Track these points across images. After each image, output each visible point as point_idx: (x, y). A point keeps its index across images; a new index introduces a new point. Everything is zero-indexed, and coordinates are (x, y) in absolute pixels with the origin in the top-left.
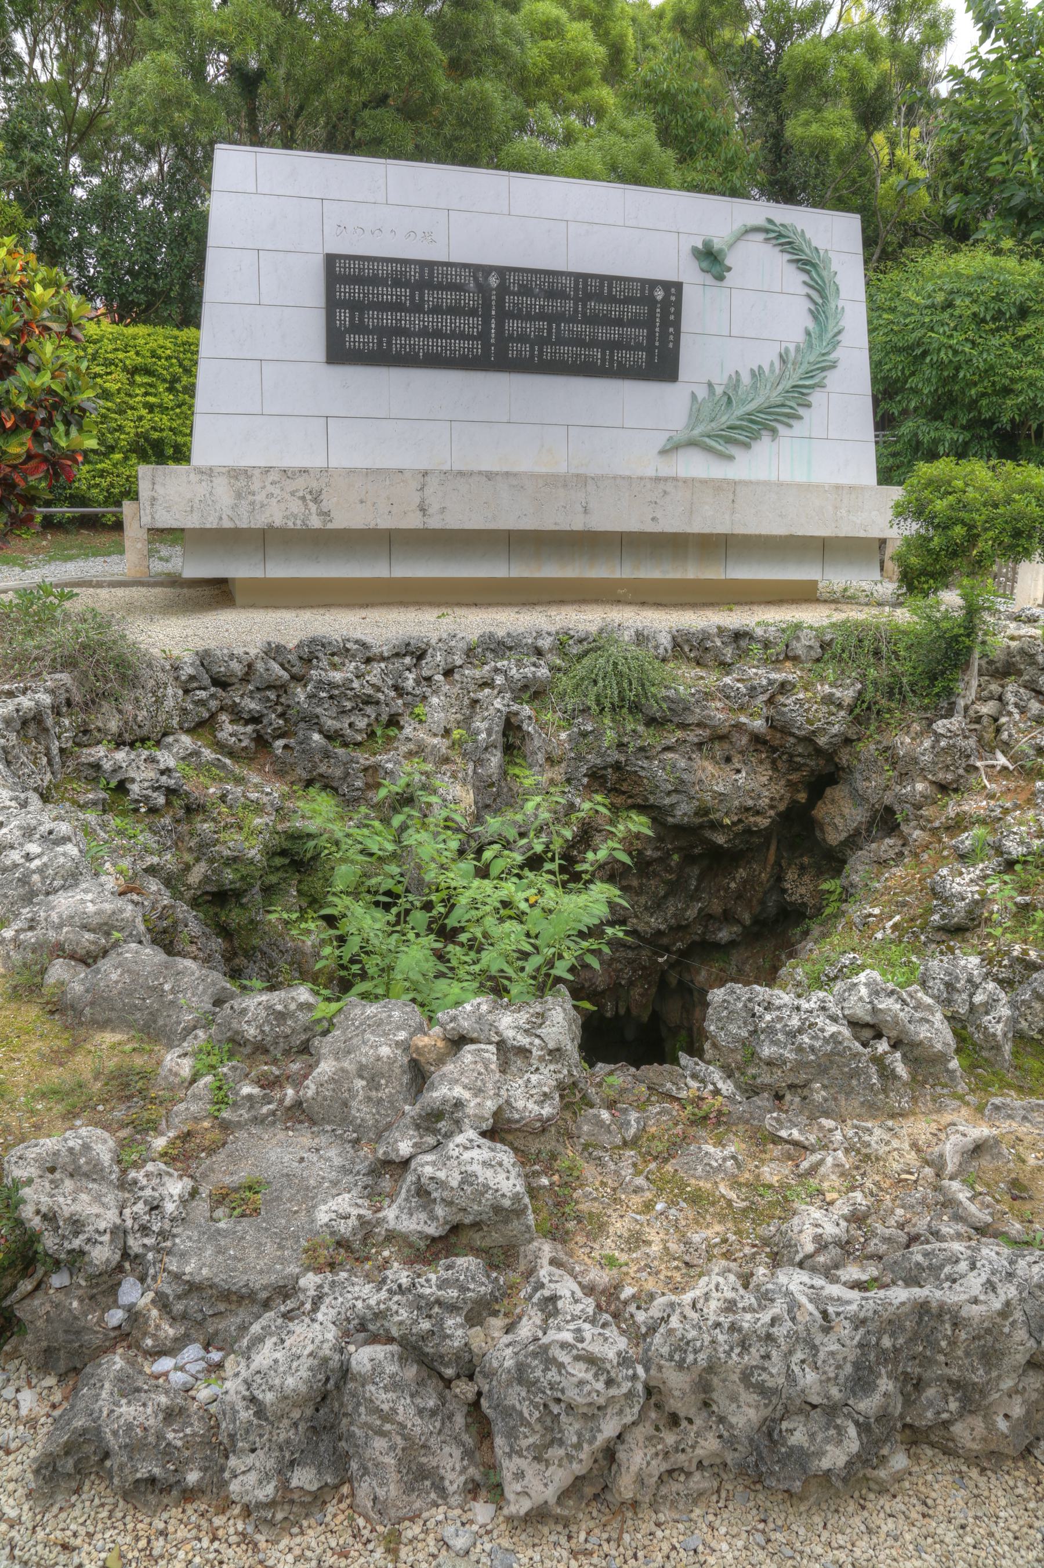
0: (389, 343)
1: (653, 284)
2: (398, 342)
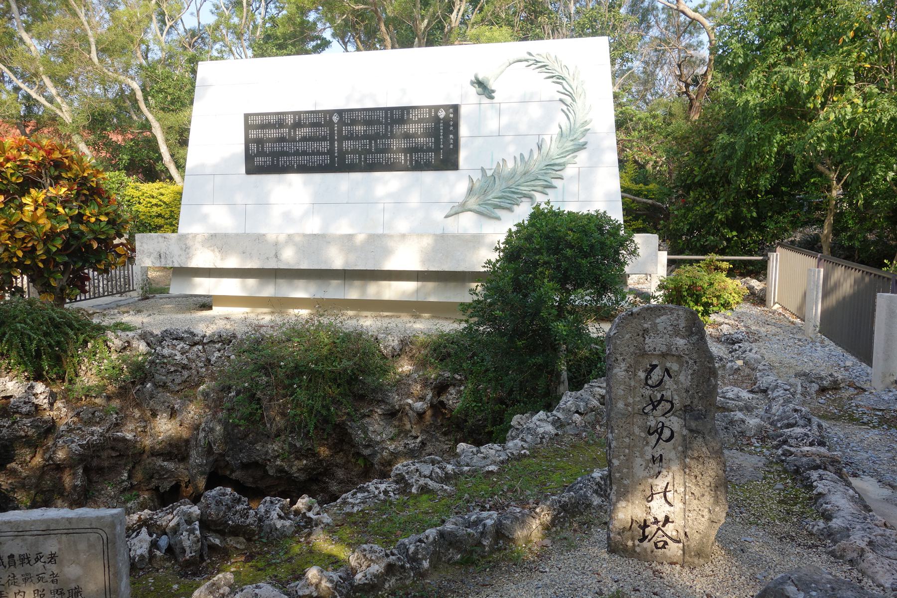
0: (278, 161)
2: (283, 160)
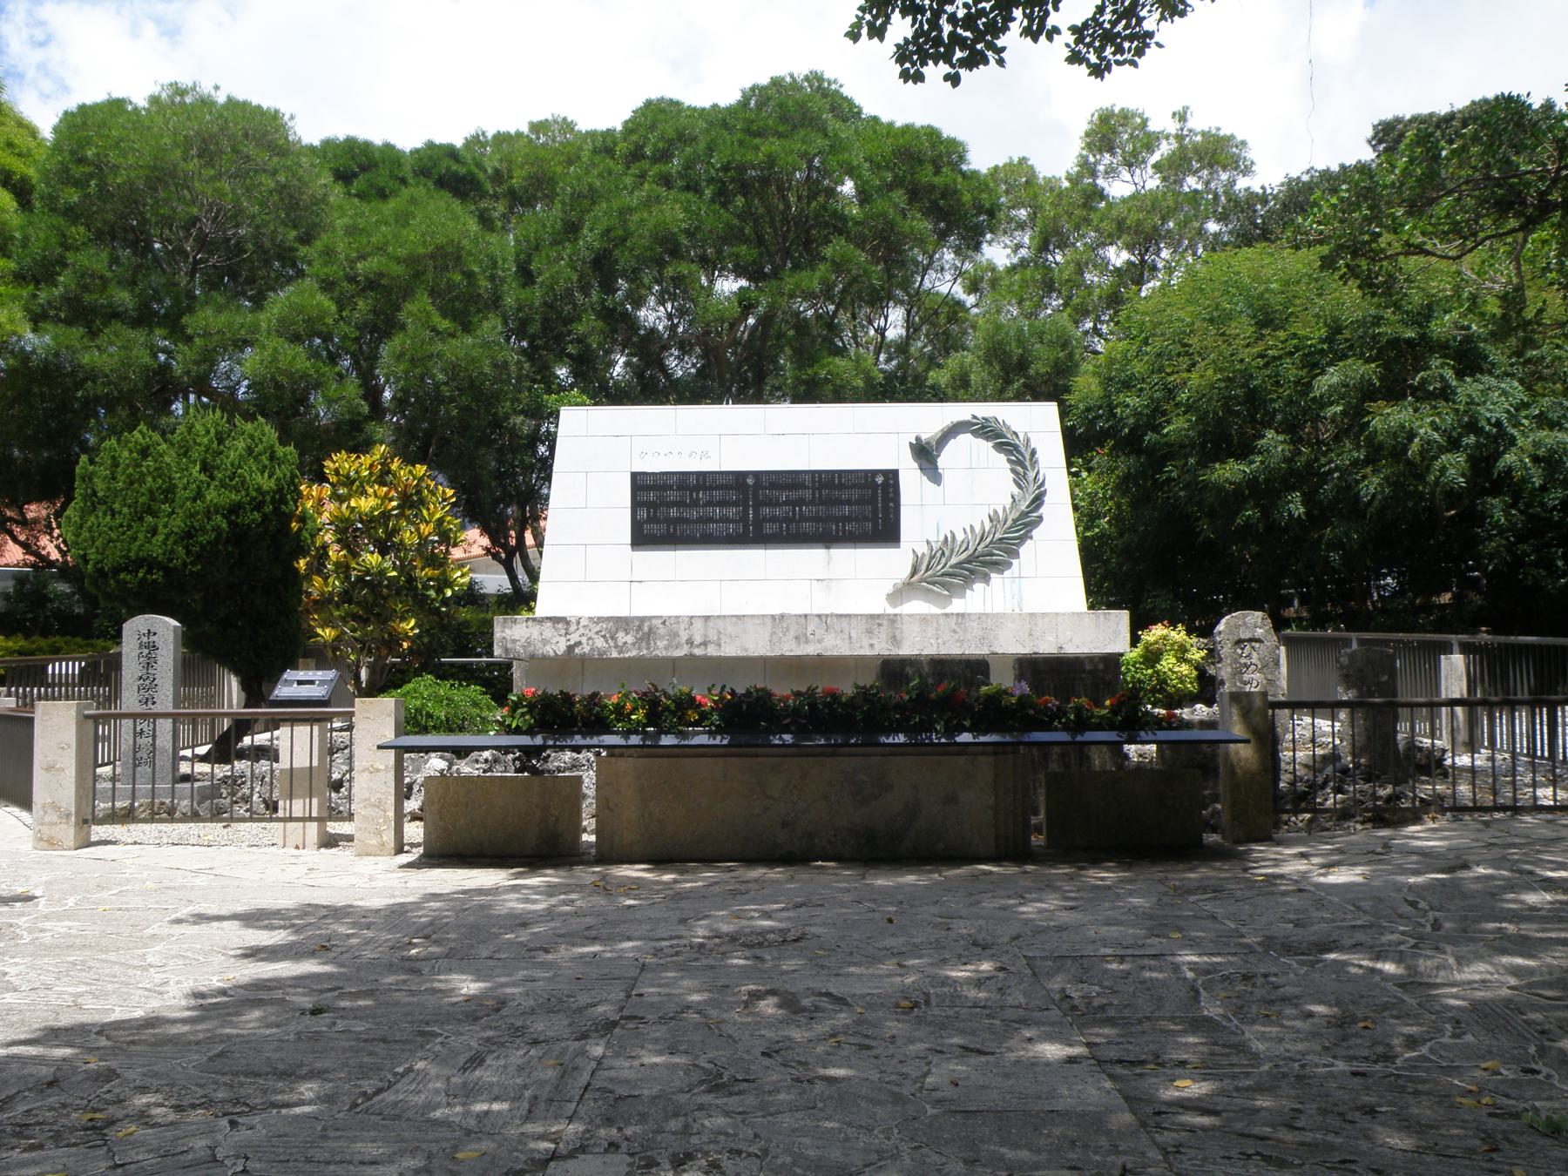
1: (875, 473)
